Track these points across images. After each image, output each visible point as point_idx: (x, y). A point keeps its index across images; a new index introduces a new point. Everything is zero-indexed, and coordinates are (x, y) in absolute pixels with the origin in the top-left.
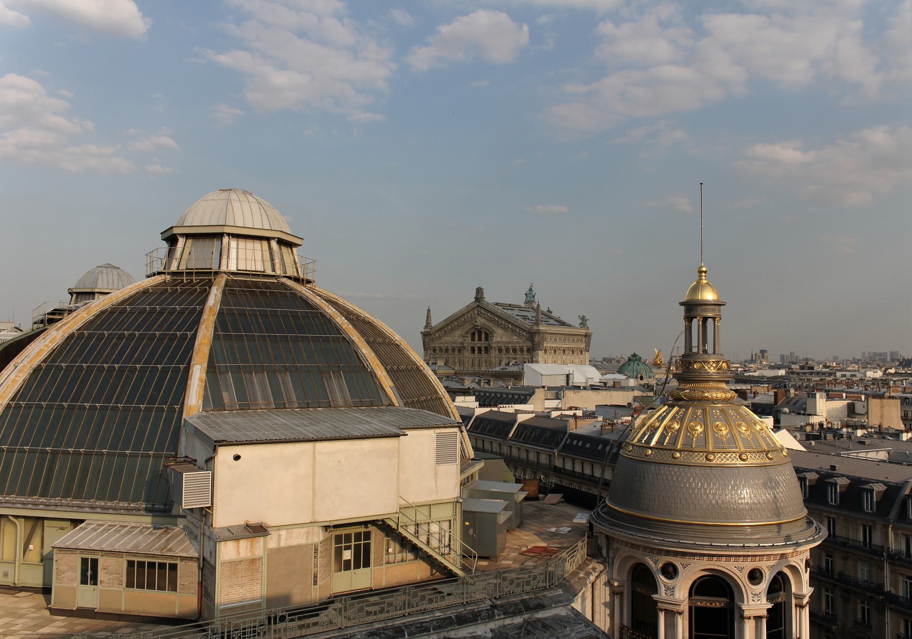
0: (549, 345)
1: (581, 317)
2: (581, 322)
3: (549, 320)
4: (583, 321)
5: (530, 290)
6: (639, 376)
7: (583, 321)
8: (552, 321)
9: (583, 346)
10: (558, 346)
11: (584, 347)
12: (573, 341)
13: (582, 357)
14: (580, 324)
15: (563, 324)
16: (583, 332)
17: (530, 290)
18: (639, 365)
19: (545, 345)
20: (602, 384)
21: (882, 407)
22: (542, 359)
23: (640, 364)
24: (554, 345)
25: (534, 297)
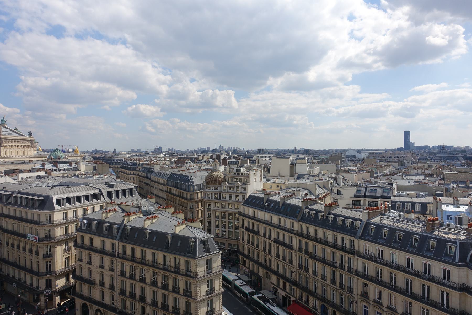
0: (7, 144)
1: (29, 132)
2: (29, 134)
3: (12, 133)
4: (30, 134)
5: (4, 118)
6: (58, 158)
7: (30, 134)
8: (14, 133)
9: (30, 145)
10: (13, 145)
11: (30, 145)
12: (23, 143)
13: (29, 149)
14: (29, 135)
15: (21, 135)
16: (30, 138)
17: (4, 118)
18: (58, 153)
19: (4, 144)
20: (23, 161)
21: (103, 167)
22: (3, 151)
23: (59, 153)
24: (10, 144)
25: (5, 122)
